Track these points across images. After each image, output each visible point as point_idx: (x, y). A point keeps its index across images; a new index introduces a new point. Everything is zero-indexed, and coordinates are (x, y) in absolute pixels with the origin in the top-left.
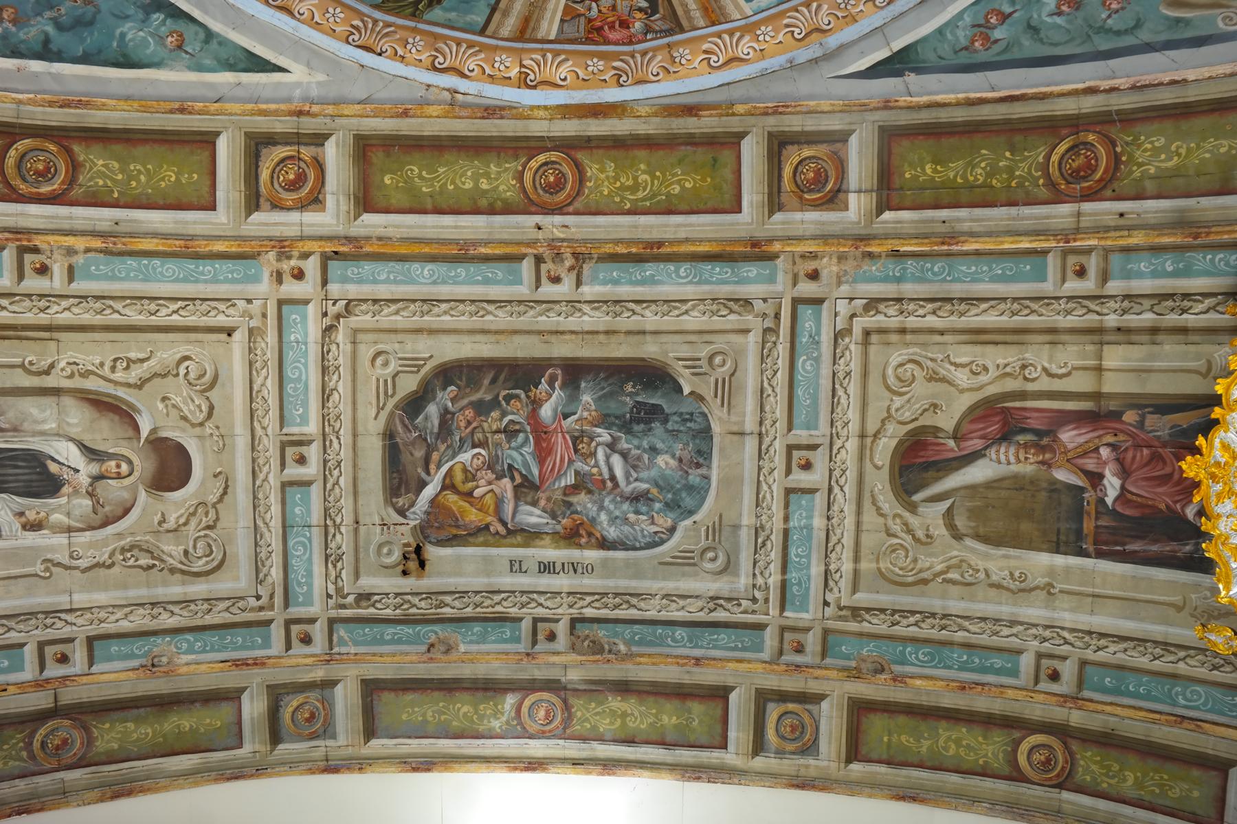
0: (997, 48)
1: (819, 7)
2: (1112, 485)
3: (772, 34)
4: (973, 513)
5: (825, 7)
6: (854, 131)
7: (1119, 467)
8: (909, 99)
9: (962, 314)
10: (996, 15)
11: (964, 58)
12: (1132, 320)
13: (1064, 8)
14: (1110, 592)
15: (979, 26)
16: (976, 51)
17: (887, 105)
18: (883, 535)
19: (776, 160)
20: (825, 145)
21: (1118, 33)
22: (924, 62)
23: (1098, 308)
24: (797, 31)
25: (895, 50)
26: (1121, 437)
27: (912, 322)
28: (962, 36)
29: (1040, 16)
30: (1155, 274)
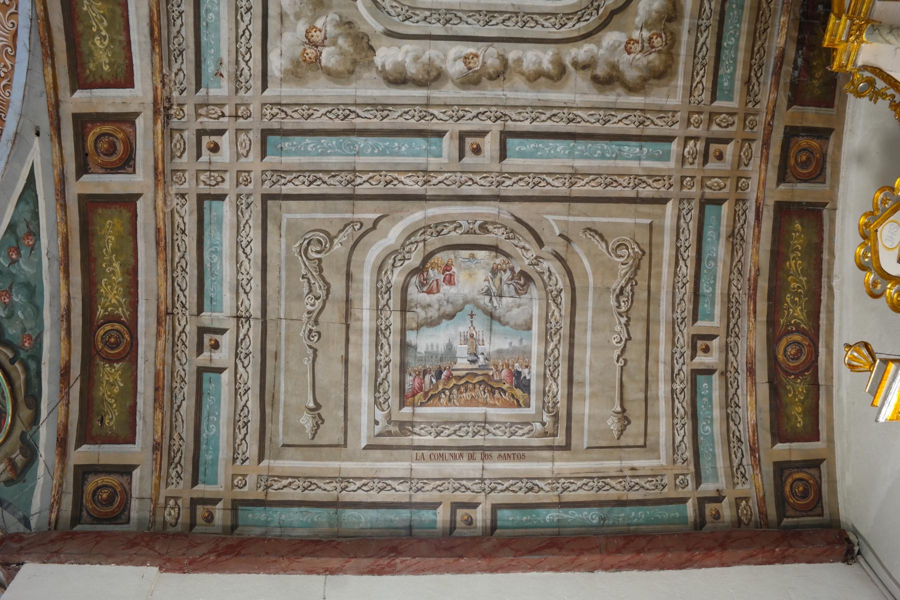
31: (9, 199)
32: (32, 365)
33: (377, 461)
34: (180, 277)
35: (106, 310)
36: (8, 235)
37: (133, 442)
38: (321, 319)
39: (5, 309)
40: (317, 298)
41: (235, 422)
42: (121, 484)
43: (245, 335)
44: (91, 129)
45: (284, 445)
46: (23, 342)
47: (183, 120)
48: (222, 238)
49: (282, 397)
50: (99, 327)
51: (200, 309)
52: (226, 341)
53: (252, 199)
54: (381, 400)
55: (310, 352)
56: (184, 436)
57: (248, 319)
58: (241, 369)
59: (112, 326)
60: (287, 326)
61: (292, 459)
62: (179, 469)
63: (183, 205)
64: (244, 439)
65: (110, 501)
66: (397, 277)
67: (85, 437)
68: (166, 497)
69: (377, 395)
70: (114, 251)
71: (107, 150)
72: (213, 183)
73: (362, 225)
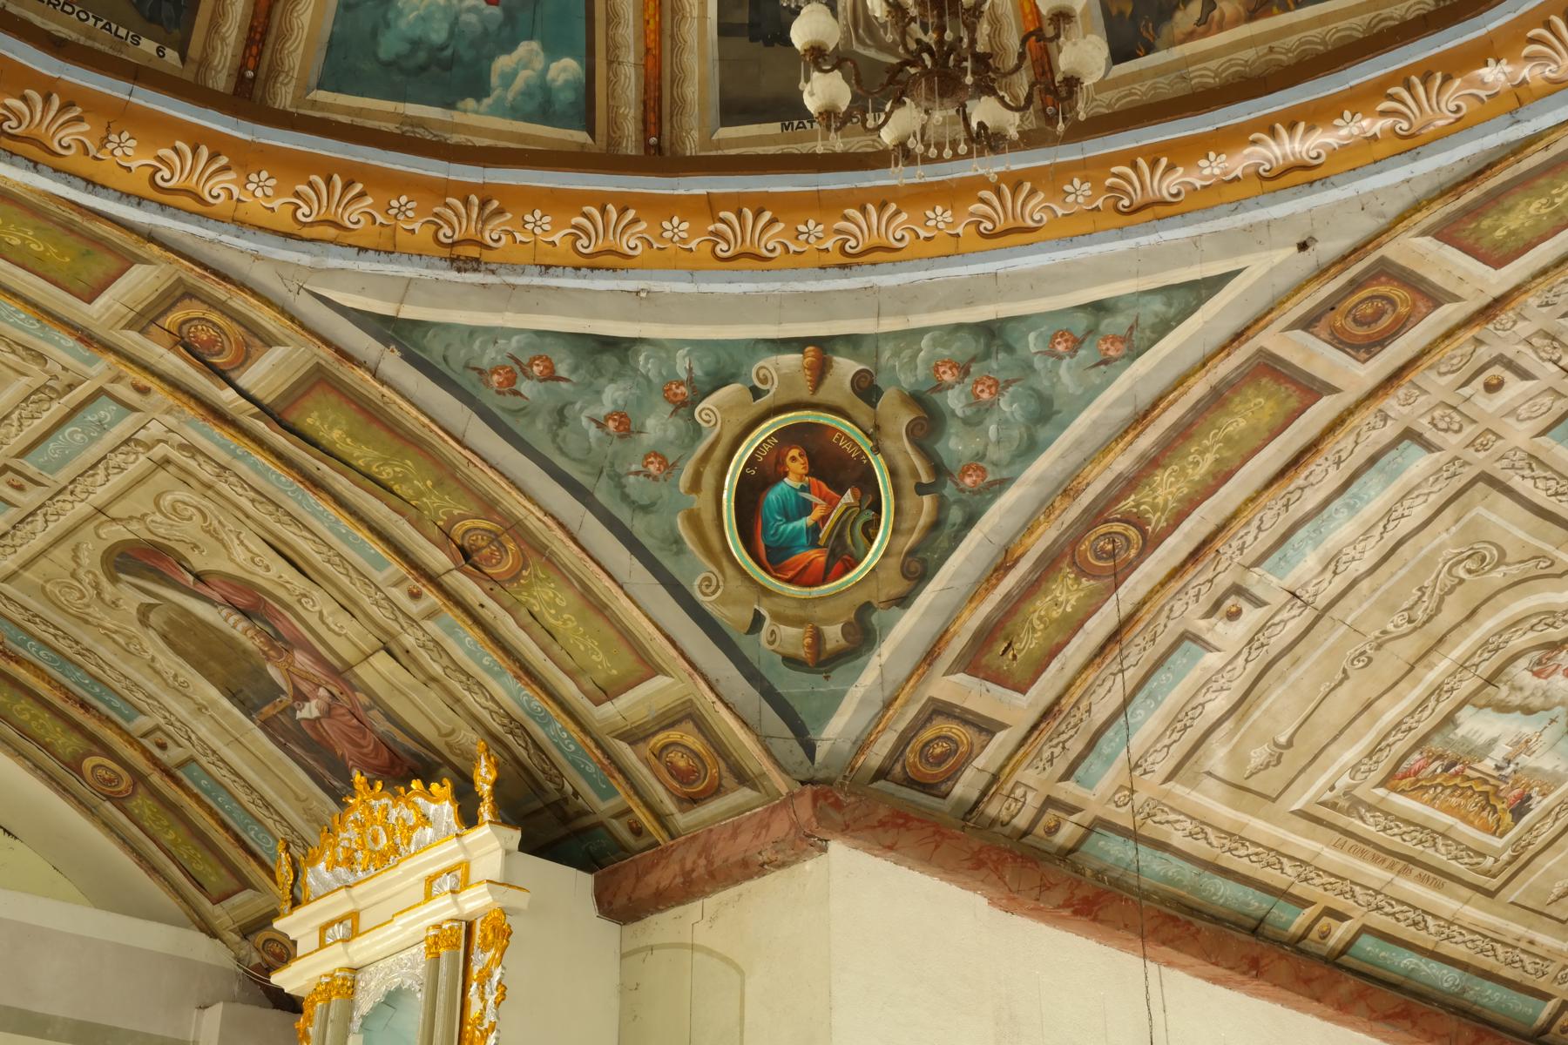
0: (510, 401)
1: (362, 195)
2: (310, 711)
3: (269, 192)
4: (171, 622)
5: (369, 200)
6: (286, 345)
7: (326, 708)
8: (368, 377)
9: (279, 521)
10: (545, 367)
11: (467, 380)
12: (424, 657)
13: (611, 424)
14: (253, 749)
15: (517, 362)
16: (487, 384)
17: (345, 355)
18: (67, 574)
19: (169, 301)
20: (241, 329)
21: (625, 497)
22: (424, 350)
23: (405, 625)
24: (306, 210)
25: (401, 315)
26: (345, 698)
27: (223, 487)
28: (490, 356)
29: (582, 410)
30: (470, 654)
31: (1138, 274)
32: (955, 515)
33: (1294, 832)
34: (1274, 512)
35: (1138, 505)
36: (1080, 315)
37: (1024, 692)
38: (1387, 646)
39: (969, 405)
40: (1410, 621)
41: (1176, 719)
42: (972, 744)
43: (1282, 621)
44: (1382, 284)
45: (1209, 774)
46: (964, 472)
47: (1499, 333)
48: (1377, 495)
49: (1256, 714)
50: (1107, 521)
51: (1258, 562)
52: (1252, 617)
53: (1466, 469)
54: (1363, 768)
55: (1339, 676)
56: (1094, 708)
57: (1306, 604)
58: (1241, 660)
59: (1126, 529)
60: (1344, 636)
61: (1205, 793)
62: (1057, 751)
63: (1374, 428)
64: (1169, 747)
65: (941, 759)
66: (1518, 641)
67: (973, 662)
68: (1017, 782)
69: (1366, 760)
70: (1228, 441)
71: (1364, 316)
72: (1443, 425)
73: (1552, 564)
